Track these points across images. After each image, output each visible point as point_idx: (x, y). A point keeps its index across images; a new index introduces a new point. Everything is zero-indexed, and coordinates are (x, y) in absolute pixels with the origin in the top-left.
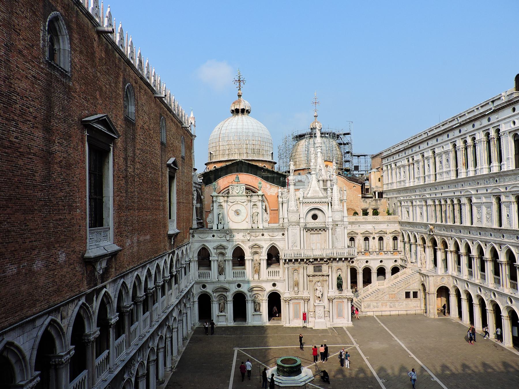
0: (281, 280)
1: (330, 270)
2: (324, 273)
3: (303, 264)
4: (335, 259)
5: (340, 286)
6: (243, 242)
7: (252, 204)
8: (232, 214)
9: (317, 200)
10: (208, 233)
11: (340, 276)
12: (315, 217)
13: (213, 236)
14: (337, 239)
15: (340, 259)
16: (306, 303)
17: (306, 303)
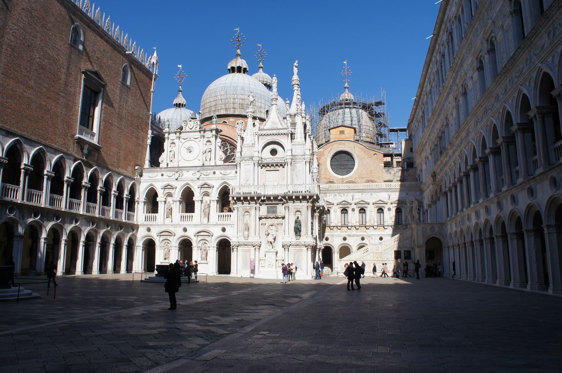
0: (236, 225)
1: (287, 211)
2: (279, 214)
3: (253, 204)
4: (290, 198)
5: (298, 231)
6: (192, 181)
7: (206, 139)
8: (184, 151)
9: (275, 132)
10: (157, 171)
11: (298, 218)
12: (274, 152)
13: (162, 175)
14: (297, 176)
15: (297, 198)
16: (257, 250)
17: (257, 250)
